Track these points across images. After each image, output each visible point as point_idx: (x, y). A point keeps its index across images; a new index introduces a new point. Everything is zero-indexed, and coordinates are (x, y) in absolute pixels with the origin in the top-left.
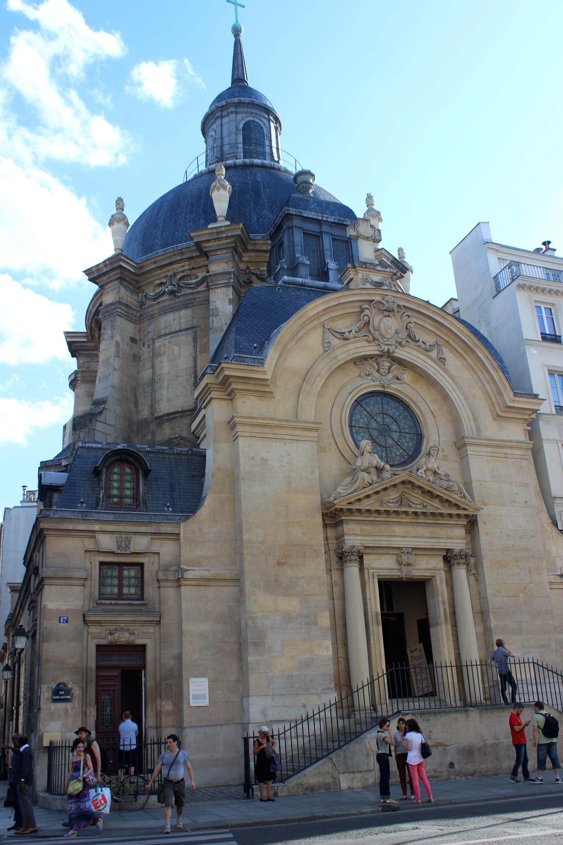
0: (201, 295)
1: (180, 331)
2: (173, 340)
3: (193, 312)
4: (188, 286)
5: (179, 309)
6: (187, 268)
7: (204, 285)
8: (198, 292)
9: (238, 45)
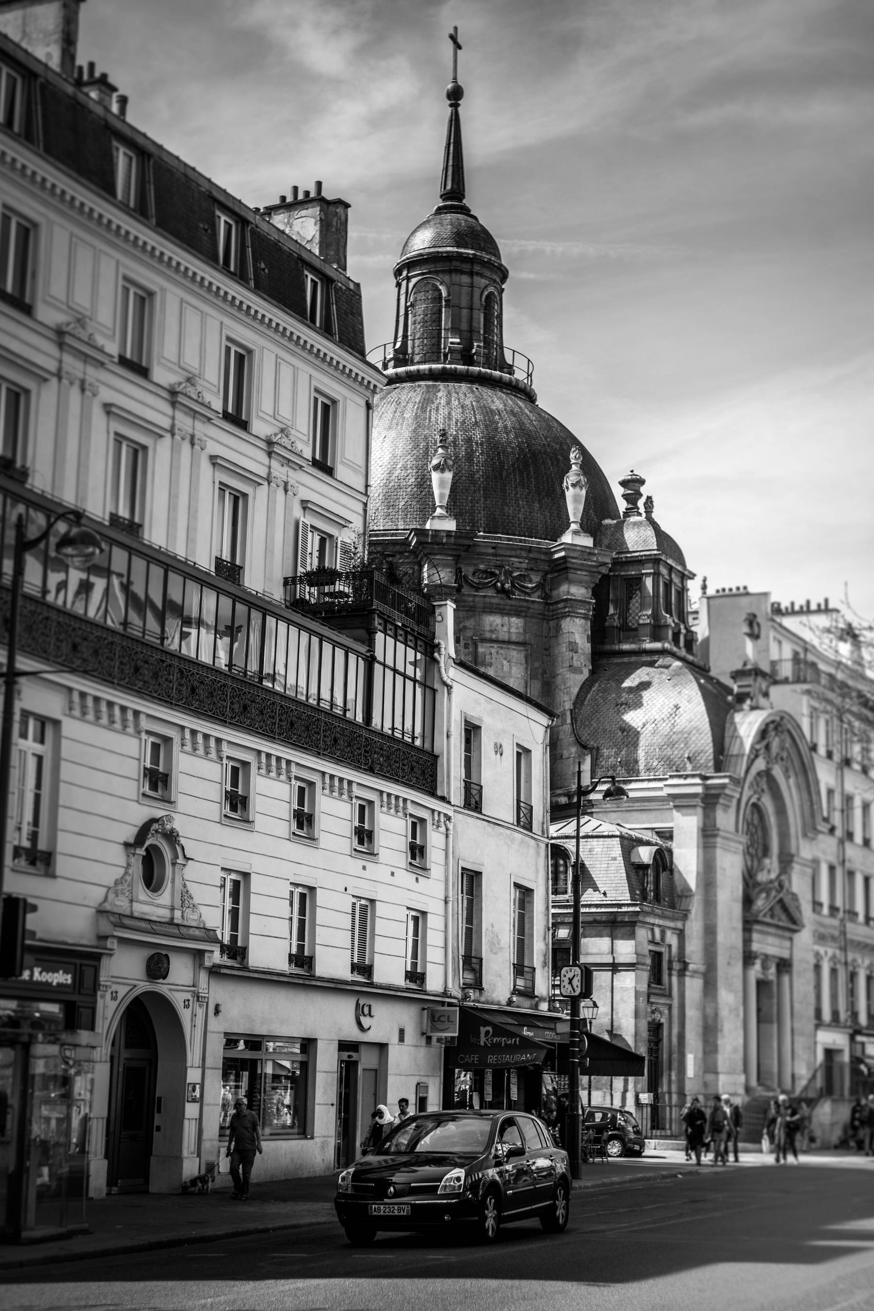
0: (536, 606)
1: (509, 642)
2: (501, 651)
3: (525, 623)
4: (523, 590)
5: (509, 614)
6: (524, 566)
7: (538, 593)
8: (534, 602)
9: (455, 123)
